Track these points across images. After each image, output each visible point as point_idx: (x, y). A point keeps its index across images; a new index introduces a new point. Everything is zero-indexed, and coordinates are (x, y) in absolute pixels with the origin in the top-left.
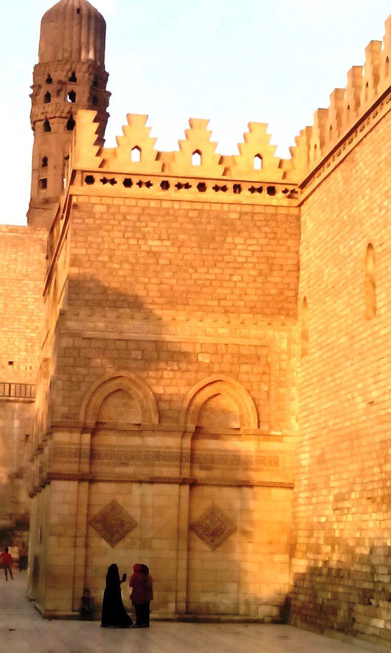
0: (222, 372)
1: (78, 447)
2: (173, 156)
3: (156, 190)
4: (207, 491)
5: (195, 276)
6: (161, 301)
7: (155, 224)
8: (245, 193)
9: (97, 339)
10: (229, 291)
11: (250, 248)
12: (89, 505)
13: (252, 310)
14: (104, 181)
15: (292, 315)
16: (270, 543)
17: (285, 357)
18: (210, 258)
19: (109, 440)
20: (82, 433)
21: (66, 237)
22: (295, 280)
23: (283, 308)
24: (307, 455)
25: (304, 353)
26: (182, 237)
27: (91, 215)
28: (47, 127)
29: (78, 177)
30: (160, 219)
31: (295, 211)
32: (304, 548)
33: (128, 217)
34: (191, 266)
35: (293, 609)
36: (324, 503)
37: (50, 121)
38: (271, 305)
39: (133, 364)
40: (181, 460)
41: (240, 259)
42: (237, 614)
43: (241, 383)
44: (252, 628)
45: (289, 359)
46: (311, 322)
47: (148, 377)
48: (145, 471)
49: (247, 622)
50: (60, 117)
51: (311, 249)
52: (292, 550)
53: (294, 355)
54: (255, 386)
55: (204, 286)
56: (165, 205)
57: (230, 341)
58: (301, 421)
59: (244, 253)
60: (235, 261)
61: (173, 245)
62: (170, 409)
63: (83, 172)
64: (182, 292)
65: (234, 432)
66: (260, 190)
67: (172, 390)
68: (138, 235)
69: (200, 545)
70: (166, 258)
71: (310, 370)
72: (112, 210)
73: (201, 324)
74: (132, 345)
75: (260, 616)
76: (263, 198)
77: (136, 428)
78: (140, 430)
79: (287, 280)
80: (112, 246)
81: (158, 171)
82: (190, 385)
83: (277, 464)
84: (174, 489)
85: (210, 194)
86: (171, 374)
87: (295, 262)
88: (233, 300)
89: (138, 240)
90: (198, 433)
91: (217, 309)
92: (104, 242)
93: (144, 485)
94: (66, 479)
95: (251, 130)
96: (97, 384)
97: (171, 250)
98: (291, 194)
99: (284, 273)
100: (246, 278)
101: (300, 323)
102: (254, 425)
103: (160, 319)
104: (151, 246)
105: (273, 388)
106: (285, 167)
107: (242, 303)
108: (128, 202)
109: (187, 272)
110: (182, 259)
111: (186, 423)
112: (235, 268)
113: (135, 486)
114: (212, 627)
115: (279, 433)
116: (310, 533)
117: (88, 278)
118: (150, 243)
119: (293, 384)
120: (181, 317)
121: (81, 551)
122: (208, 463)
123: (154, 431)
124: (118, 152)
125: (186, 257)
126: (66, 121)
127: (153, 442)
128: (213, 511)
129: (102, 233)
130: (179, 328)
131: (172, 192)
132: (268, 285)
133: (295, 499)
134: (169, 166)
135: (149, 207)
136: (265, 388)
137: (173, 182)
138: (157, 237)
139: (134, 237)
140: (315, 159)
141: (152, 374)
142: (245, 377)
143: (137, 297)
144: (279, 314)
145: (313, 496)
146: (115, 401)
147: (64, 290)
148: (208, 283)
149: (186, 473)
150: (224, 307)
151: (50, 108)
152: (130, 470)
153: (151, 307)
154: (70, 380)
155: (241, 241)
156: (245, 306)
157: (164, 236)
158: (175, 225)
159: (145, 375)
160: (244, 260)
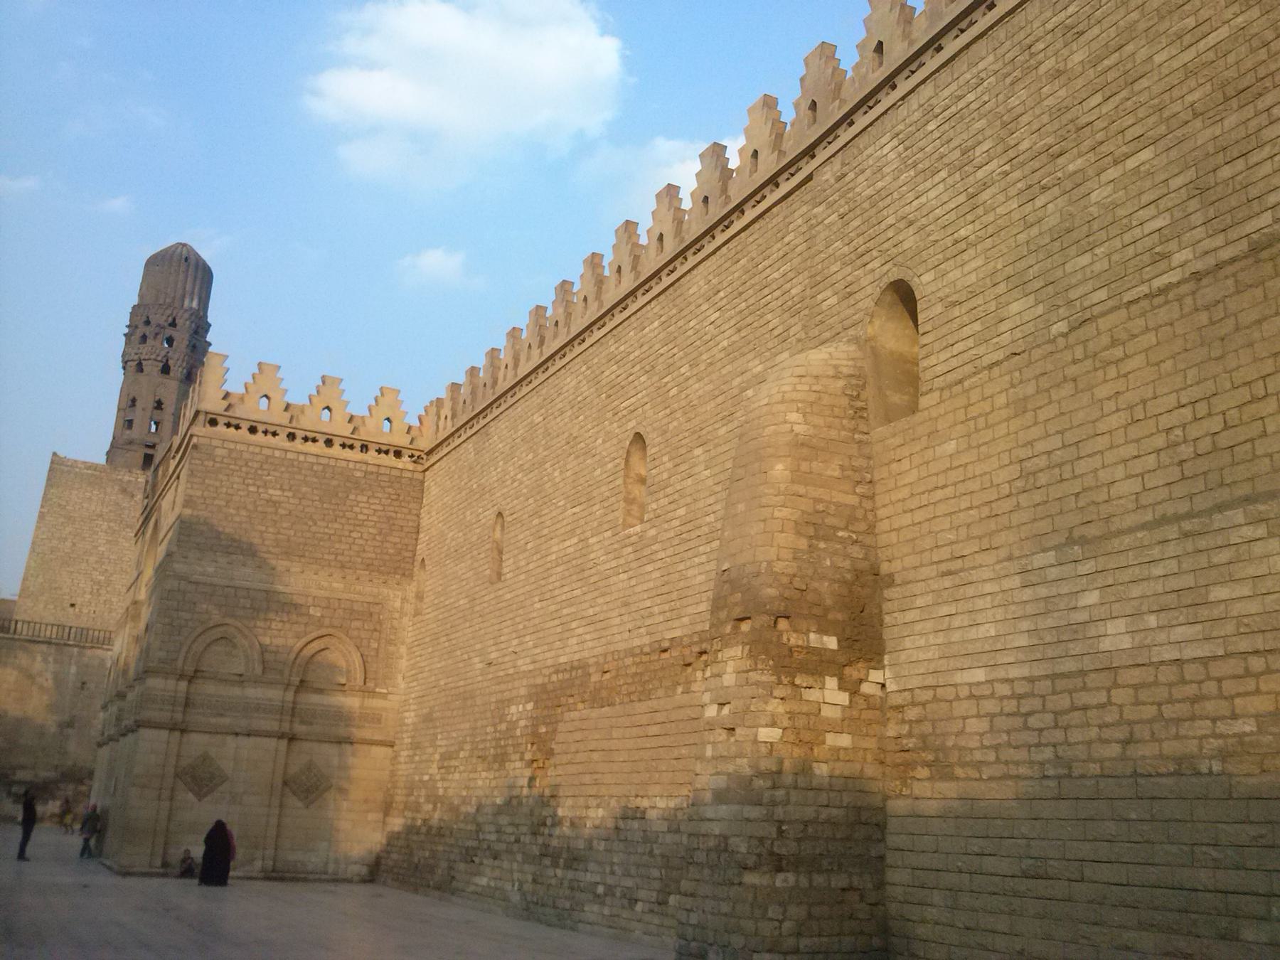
0: (333, 627)
1: (173, 694)
2: (302, 409)
3: (280, 440)
4: (306, 746)
5: (314, 529)
7: (277, 474)
8: (372, 453)
9: (205, 584)
10: (348, 546)
11: (373, 507)
12: (178, 756)
13: (368, 566)
14: (228, 425)
15: (408, 575)
16: (366, 801)
17: (397, 615)
18: (331, 512)
19: (209, 688)
20: (178, 680)
21: (178, 477)
22: (414, 542)
24: (413, 714)
25: (417, 613)
26: (304, 489)
27: (212, 457)
28: (140, 368)
29: (201, 417)
30: (283, 469)
31: (420, 476)
32: (401, 807)
33: (250, 464)
34: (311, 518)
35: (383, 867)
36: (427, 761)
37: (144, 363)
38: (388, 564)
40: (282, 713)
41: (361, 517)
42: (326, 873)
43: (351, 638)
44: (342, 888)
45: (401, 618)
46: (428, 583)
47: (255, 627)
49: (336, 881)
50: (155, 360)
51: (434, 513)
52: (387, 809)
53: (406, 615)
54: (365, 643)
55: (321, 540)
56: (290, 456)
57: (345, 596)
58: (408, 680)
59: (366, 511)
60: (356, 519)
61: (294, 497)
62: (275, 661)
63: (207, 413)
64: (300, 544)
65: (341, 688)
66: (387, 452)
67: (280, 641)
68: (258, 483)
69: (293, 802)
70: (285, 509)
71: (423, 630)
72: (234, 455)
73: (315, 577)
75: (349, 876)
76: (390, 460)
77: (237, 678)
78: (241, 680)
79: (406, 541)
80: (230, 491)
82: (298, 637)
83: (379, 721)
84: (272, 743)
85: (336, 450)
86: (280, 625)
87: (415, 525)
88: (351, 557)
89: (258, 487)
90: (303, 685)
91: (333, 564)
92: (222, 486)
93: (240, 738)
94: (155, 727)
95: (382, 394)
96: (199, 630)
97: (292, 501)
98: (416, 460)
99: (403, 534)
100: (365, 536)
101: (415, 584)
102: (360, 681)
103: (273, 569)
104: (271, 495)
105: (383, 646)
106: (413, 433)
107: (359, 560)
108: (251, 449)
109: (306, 524)
110: (303, 511)
111: (290, 675)
112: (355, 525)
113: (229, 739)
115: (385, 691)
116: (410, 789)
117: (202, 520)
118: (271, 492)
119: (403, 643)
120: (296, 568)
121: (166, 804)
123: (257, 682)
125: (307, 510)
126: (161, 365)
127: (253, 693)
129: (220, 476)
130: (292, 580)
131: (298, 444)
132: (388, 545)
133: (395, 758)
134: (298, 421)
135: (273, 457)
137: (300, 434)
138: (278, 486)
139: (254, 485)
140: (445, 429)
141: (259, 623)
142: (355, 633)
143: (251, 544)
144: (395, 573)
145: (415, 755)
147: (170, 534)
148: (326, 537)
149: (286, 727)
150: (340, 562)
151: (145, 350)
152: (226, 721)
153: (266, 556)
154: (170, 624)
155: (365, 499)
156: (362, 563)
157: (286, 487)
159: (252, 624)
160: (365, 517)
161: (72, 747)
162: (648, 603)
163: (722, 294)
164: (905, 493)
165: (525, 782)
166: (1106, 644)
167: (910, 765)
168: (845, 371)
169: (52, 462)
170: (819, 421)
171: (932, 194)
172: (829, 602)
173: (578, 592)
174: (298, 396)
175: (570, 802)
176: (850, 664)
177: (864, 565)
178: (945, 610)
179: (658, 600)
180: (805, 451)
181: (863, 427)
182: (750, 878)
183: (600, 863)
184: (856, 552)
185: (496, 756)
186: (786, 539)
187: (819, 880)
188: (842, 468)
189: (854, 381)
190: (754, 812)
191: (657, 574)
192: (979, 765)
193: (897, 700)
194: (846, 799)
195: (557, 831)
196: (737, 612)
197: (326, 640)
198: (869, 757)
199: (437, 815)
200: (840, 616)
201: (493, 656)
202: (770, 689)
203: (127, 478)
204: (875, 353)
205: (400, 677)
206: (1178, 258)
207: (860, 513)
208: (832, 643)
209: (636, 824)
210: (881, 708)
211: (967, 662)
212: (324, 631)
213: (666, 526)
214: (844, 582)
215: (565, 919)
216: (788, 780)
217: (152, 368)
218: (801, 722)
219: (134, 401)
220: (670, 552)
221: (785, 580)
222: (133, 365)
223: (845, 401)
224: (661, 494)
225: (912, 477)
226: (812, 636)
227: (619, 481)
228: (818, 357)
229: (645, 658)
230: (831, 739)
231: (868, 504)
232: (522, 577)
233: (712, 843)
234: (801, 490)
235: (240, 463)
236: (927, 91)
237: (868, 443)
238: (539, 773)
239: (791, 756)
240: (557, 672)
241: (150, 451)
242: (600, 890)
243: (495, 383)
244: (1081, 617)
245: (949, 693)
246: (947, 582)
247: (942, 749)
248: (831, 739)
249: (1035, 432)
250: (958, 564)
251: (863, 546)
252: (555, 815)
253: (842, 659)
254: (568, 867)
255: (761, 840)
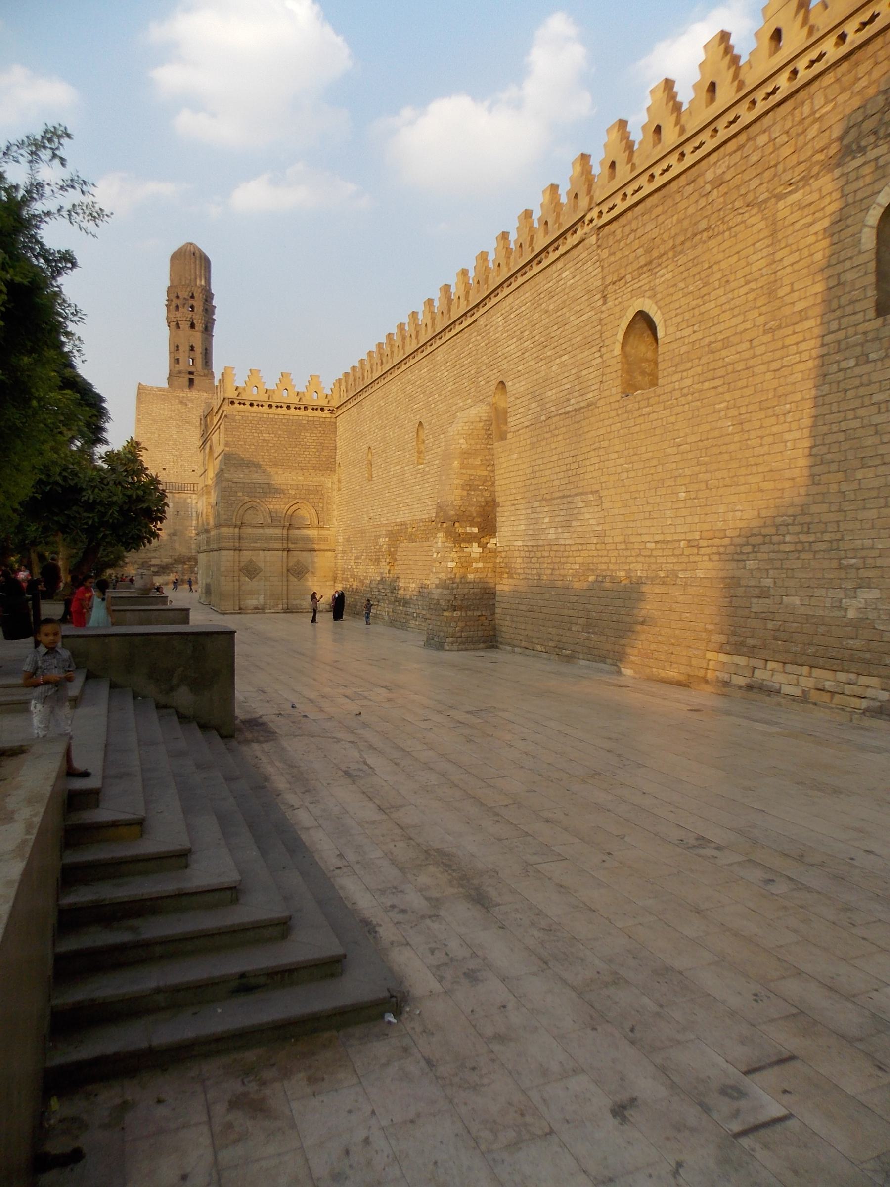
2: (274, 391)
3: (265, 409)
6: (271, 464)
8: (310, 410)
13: (314, 468)
14: (240, 403)
16: (325, 576)
17: (330, 491)
21: (219, 428)
23: (328, 467)
25: (339, 490)
27: (235, 421)
29: (227, 401)
39: (258, 495)
48: (265, 545)
52: (335, 580)
55: (290, 457)
57: (305, 483)
67: (276, 507)
68: (258, 431)
69: (292, 578)
74: (257, 485)
76: (318, 413)
78: (262, 526)
81: (266, 399)
98: (332, 411)
108: (252, 415)
113: (261, 552)
114: (299, 615)
116: (344, 572)
122: (295, 541)
123: (269, 526)
124: (246, 389)
126: (189, 323)
127: (269, 531)
128: (298, 562)
132: (321, 456)
136: (321, 505)
146: (249, 512)
147: (220, 458)
149: (285, 546)
151: (179, 315)
152: (258, 545)
158: (276, 426)
161: (177, 546)
162: (427, 500)
163: (448, 364)
164: (502, 471)
165: (387, 571)
166: (550, 537)
167: (502, 573)
168: (484, 419)
169: (139, 388)
170: (473, 442)
171: (512, 347)
172: (475, 515)
173: (402, 491)
174: (271, 384)
175: (403, 580)
176: (483, 537)
177: (489, 499)
178: (512, 518)
179: (430, 499)
180: (466, 455)
181: (491, 442)
182: (446, 614)
183: (415, 605)
184: (486, 494)
185: (376, 559)
186: (458, 492)
187: (469, 613)
188: (481, 461)
189: (487, 423)
190: (446, 591)
191: (429, 489)
192: (519, 574)
193: (500, 549)
194: (480, 585)
195: (400, 592)
196: (442, 519)
197: (299, 504)
198: (490, 570)
199: (355, 583)
200: (479, 520)
201: (372, 515)
202: (452, 548)
203: (182, 395)
204: (496, 408)
205: (334, 519)
206: (572, 401)
207: (488, 479)
208: (475, 530)
209: (425, 590)
210: (494, 552)
211: (517, 538)
212: (296, 501)
213: (432, 467)
214: (481, 506)
215: (404, 626)
216: (458, 580)
217: (185, 326)
218: (463, 560)
219: (178, 346)
220: (434, 479)
221: (458, 508)
222: (175, 325)
223: (484, 432)
224: (430, 453)
225: (505, 466)
226: (468, 528)
227: (415, 443)
228: (473, 411)
229: (427, 524)
230: (475, 565)
231: (492, 474)
232: (381, 480)
233: (435, 602)
234: (464, 471)
235: (248, 422)
236: (510, 299)
237: (492, 449)
238: (392, 568)
239: (459, 572)
240: (396, 525)
241: (191, 377)
242: (415, 615)
243: (363, 378)
244: (544, 526)
245: (512, 548)
246: (513, 508)
247: (510, 568)
248: (475, 565)
249: (536, 457)
250: (515, 502)
251: (490, 491)
252: (398, 586)
253: (480, 536)
254: (404, 606)
255: (449, 601)
